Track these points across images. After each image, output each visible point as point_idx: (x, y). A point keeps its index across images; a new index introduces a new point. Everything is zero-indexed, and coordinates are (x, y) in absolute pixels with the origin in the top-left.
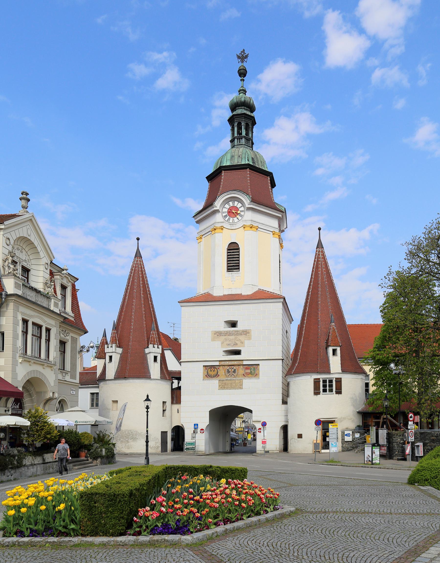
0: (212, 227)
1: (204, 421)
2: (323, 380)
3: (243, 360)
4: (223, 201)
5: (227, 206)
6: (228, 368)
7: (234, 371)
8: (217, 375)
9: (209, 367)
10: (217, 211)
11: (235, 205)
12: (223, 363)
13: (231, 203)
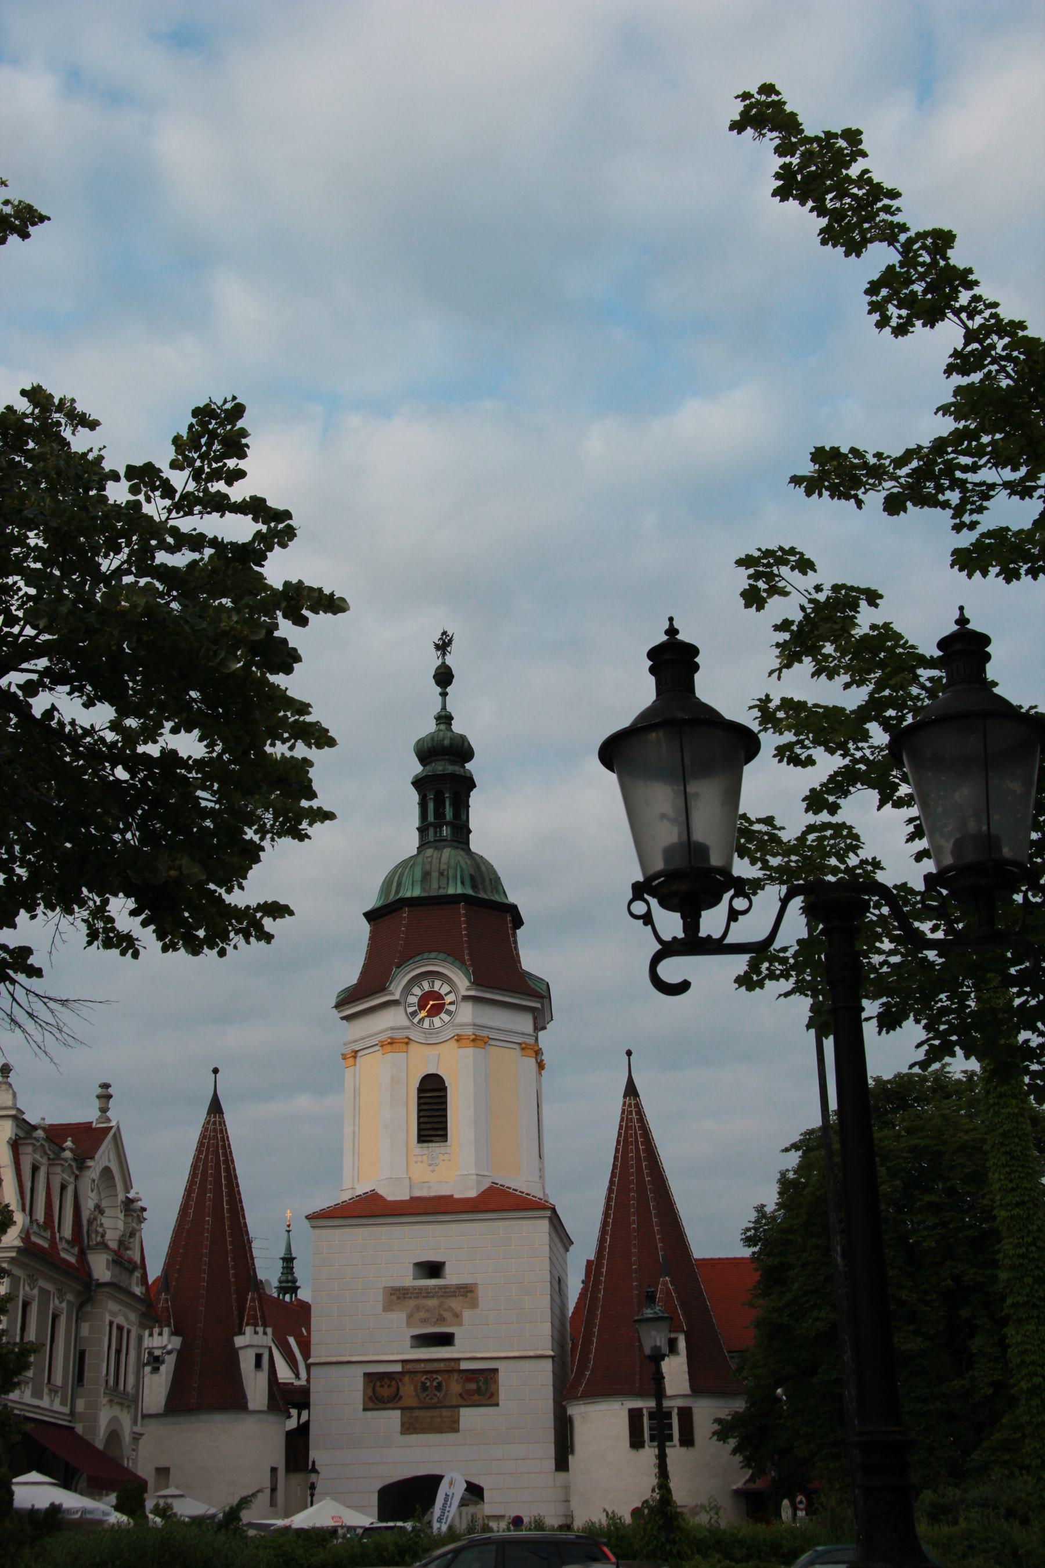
0: (383, 1037)
3: (459, 1360)
5: (417, 991)
6: (423, 1379)
7: (439, 1387)
10: (395, 1003)
11: (436, 989)
12: (410, 1367)
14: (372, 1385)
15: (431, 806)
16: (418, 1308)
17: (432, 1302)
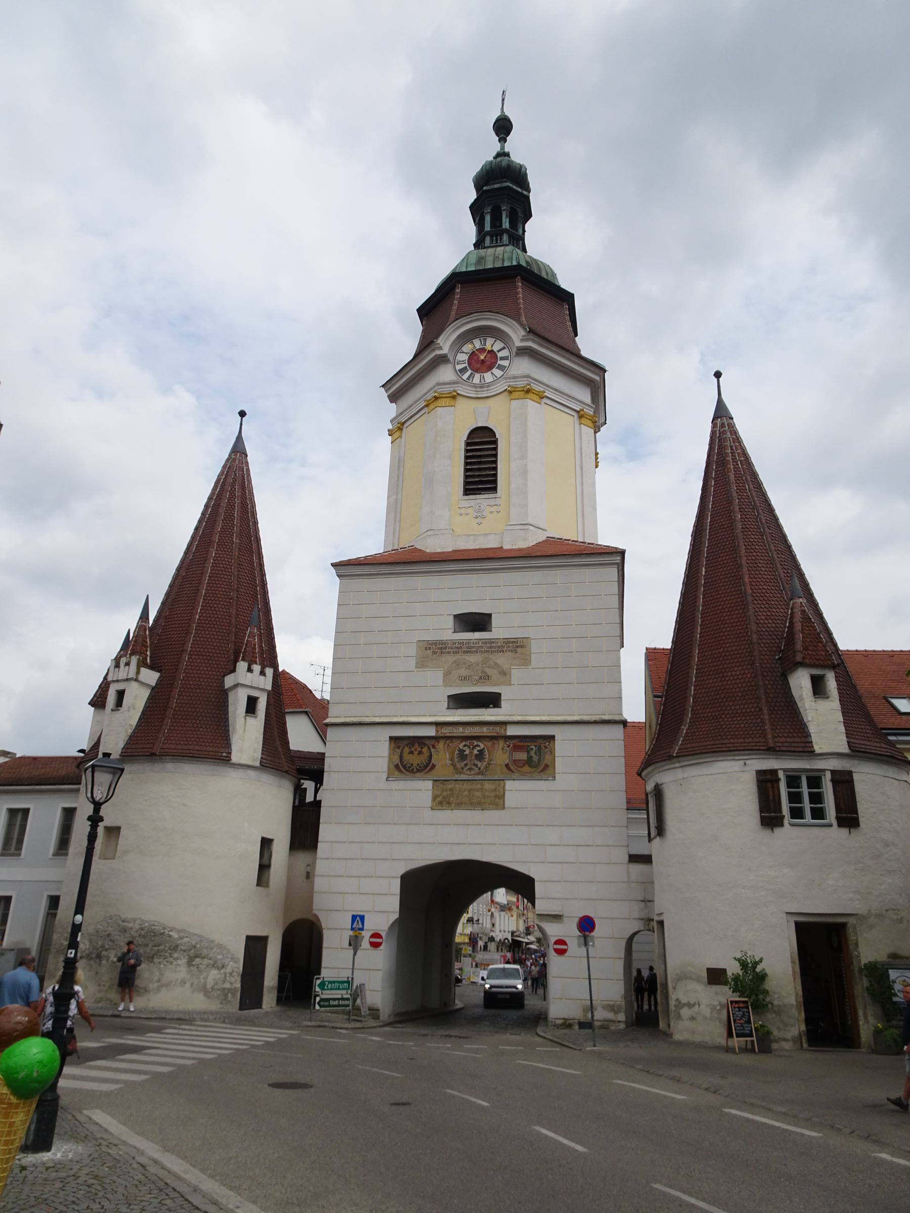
1: (384, 908)
2: (787, 777)
3: (504, 724)
4: (459, 337)
6: (461, 746)
7: (480, 756)
8: (426, 768)
9: (405, 742)
10: (442, 360)
12: (446, 731)
13: (477, 344)
14: (399, 751)
15: (488, 219)
16: (457, 664)
17: (473, 658)
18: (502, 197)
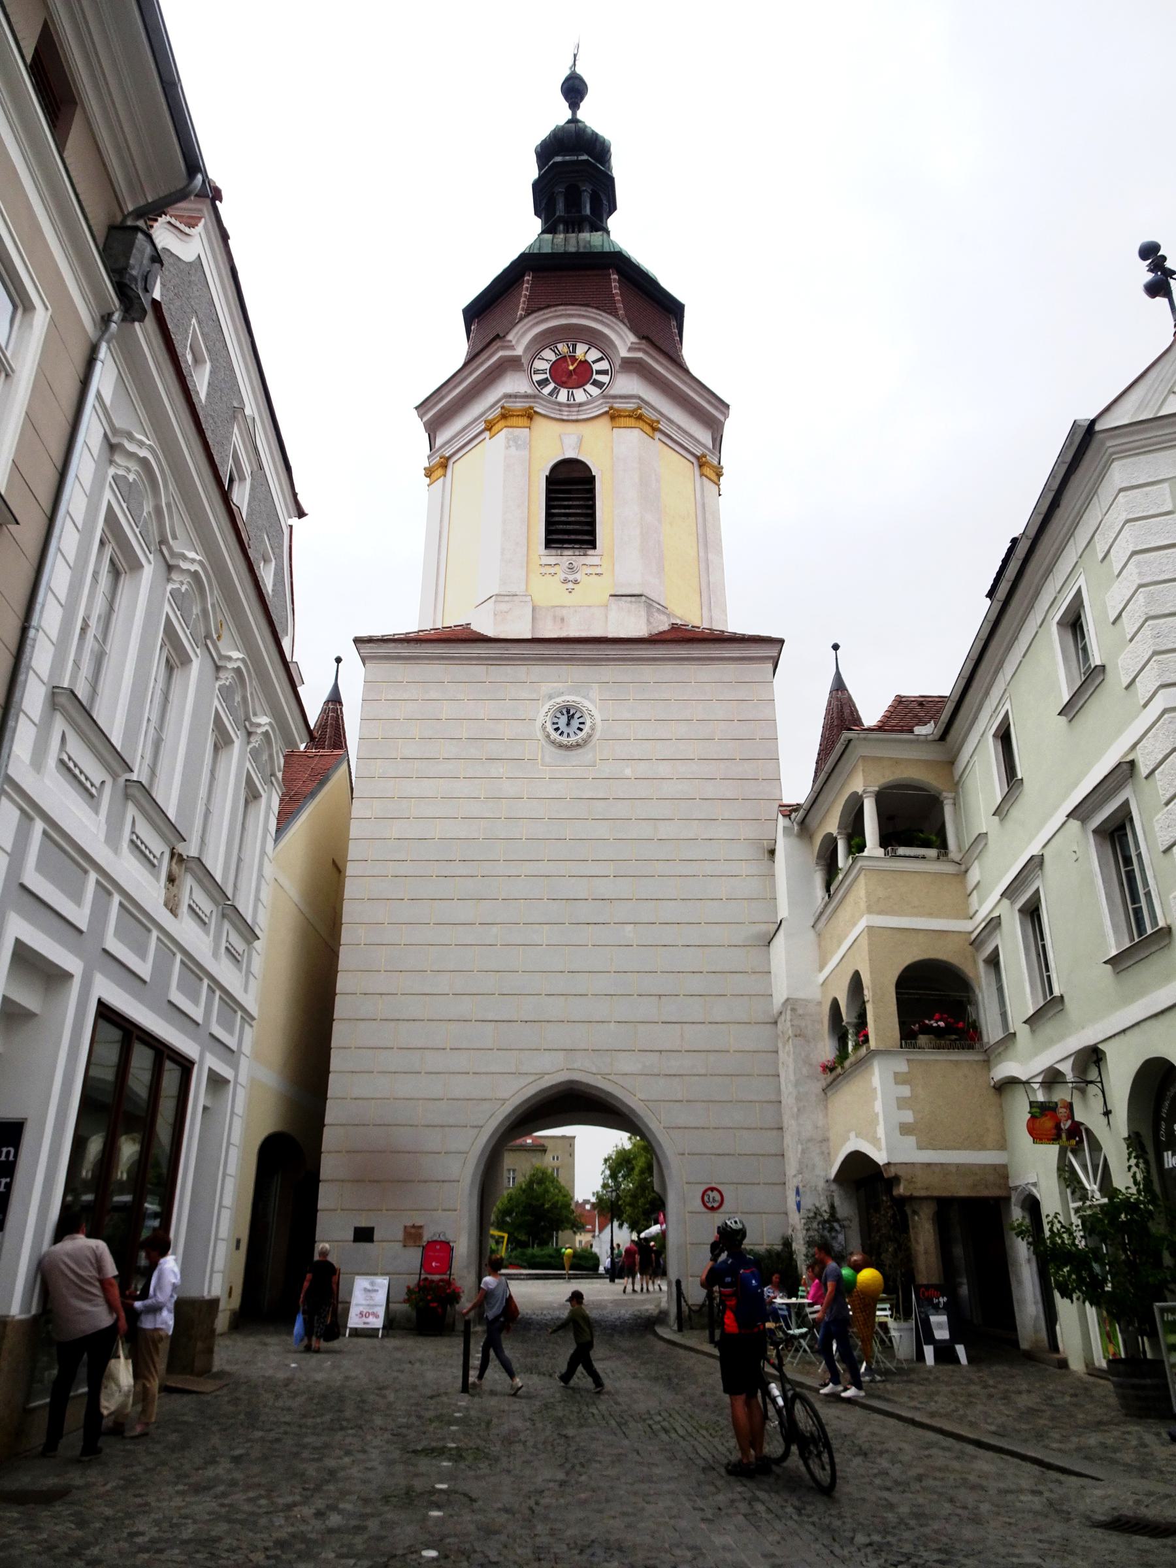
10: (514, 364)
18: (574, 175)
